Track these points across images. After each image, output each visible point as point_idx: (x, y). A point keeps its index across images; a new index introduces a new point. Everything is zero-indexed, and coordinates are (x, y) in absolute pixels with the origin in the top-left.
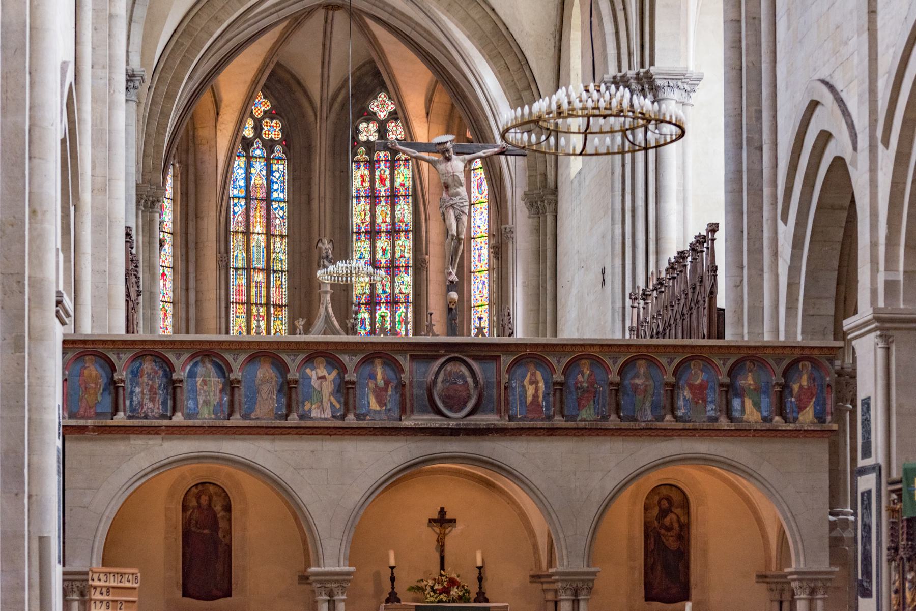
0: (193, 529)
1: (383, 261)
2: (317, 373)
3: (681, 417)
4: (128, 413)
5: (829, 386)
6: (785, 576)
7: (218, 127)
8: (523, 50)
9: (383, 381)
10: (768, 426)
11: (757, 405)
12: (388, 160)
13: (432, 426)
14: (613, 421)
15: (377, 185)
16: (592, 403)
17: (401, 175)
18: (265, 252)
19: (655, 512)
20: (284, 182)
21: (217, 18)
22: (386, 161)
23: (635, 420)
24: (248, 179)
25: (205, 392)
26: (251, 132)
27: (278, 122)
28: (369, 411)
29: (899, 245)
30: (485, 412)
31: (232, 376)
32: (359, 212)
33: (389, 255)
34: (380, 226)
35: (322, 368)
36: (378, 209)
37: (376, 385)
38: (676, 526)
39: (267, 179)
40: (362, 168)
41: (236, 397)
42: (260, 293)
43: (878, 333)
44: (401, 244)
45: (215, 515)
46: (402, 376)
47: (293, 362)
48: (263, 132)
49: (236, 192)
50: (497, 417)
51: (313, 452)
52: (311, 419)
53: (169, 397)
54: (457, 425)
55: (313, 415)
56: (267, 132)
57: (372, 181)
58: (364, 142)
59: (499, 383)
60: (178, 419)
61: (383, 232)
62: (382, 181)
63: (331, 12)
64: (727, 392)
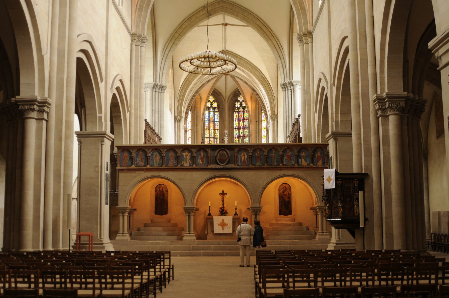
0: (158, 196)
1: (241, 135)
2: (185, 154)
3: (284, 164)
4: (135, 165)
5: (326, 155)
6: (316, 208)
7: (201, 104)
8: (269, 81)
9: (203, 156)
10: (309, 166)
11: (306, 161)
13: (216, 168)
14: (266, 166)
16: (260, 161)
19: (282, 191)
21: (195, 76)
22: (242, 111)
23: (272, 165)
24: (209, 116)
25: (156, 159)
28: (199, 164)
29: (339, 113)
30: (231, 164)
31: (163, 155)
32: (236, 124)
33: (243, 134)
35: (187, 153)
37: (201, 157)
38: (288, 194)
40: (236, 113)
41: (164, 160)
43: (333, 138)
45: (164, 192)
46: (208, 154)
47: (179, 151)
50: (234, 165)
51: (184, 175)
52: (184, 166)
53: (146, 161)
54: (223, 167)
55: (184, 165)
57: (239, 116)
58: (237, 107)
59: (234, 156)
60: (148, 166)
62: (241, 116)
63: (226, 76)
64: (297, 157)
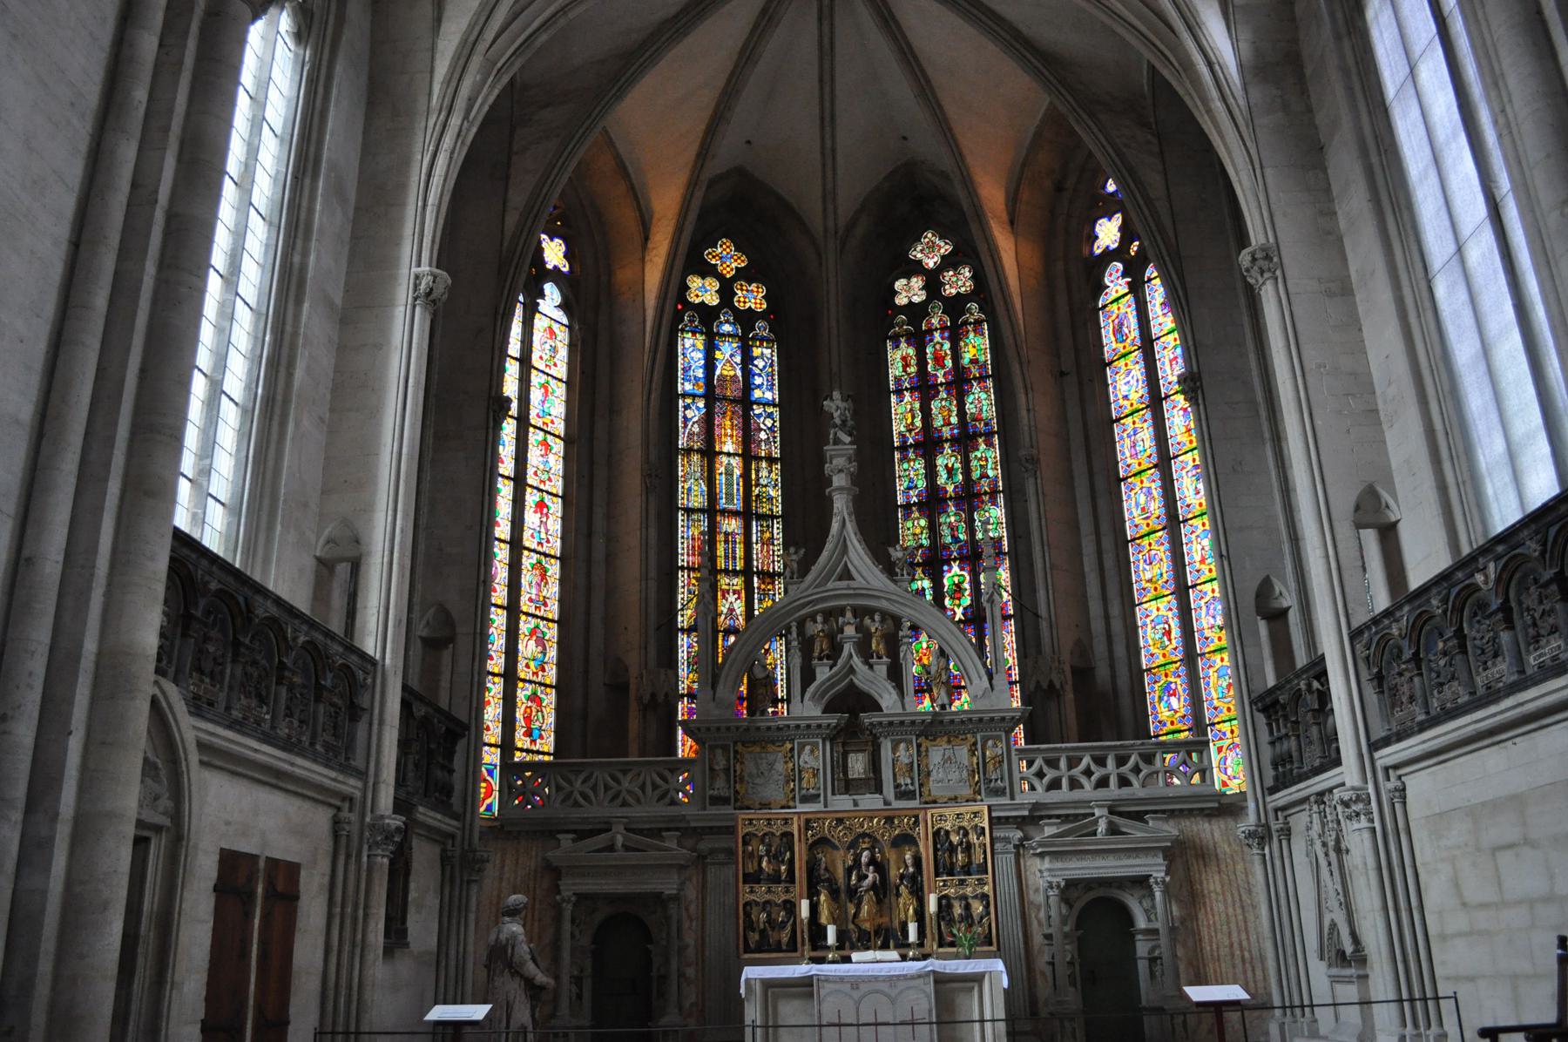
1: (950, 488)
7: (647, 258)
12: (947, 327)
15: (930, 368)
17: (970, 346)
18: (741, 484)
20: (773, 375)
22: (943, 329)
32: (903, 414)
34: (940, 431)
39: (743, 370)
40: (903, 345)
42: (734, 552)
44: (979, 456)
48: (735, 299)
49: (688, 387)
57: (922, 362)
61: (947, 440)
62: (939, 360)
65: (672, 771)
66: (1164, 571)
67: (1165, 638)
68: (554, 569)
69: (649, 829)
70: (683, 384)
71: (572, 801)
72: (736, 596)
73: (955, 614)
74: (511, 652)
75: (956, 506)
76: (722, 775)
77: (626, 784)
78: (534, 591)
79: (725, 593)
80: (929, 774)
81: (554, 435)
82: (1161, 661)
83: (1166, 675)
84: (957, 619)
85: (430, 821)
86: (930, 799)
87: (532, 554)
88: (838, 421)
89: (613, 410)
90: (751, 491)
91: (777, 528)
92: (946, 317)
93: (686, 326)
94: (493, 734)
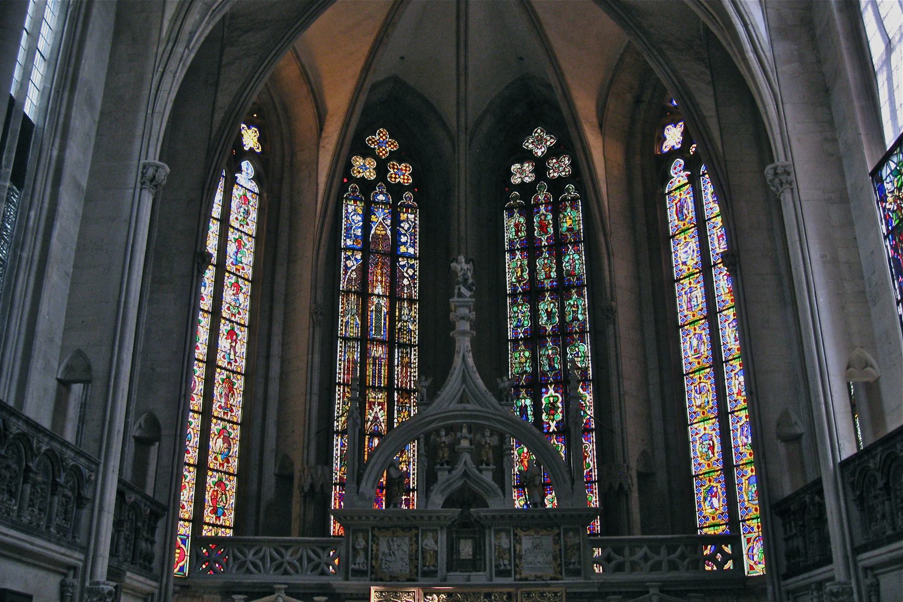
1: (549, 328)
7: (321, 144)
17: (568, 218)
18: (387, 319)
20: (415, 235)
24: (367, 225)
26: (372, 174)
27: (408, 165)
36: (539, 263)
40: (516, 215)
42: (380, 372)
49: (349, 242)
56: (393, 176)
61: (547, 290)
62: (543, 228)
65: (324, 549)
66: (710, 400)
67: (710, 452)
68: (239, 383)
69: (304, 594)
70: (345, 240)
71: (244, 569)
72: (380, 407)
73: (550, 426)
74: (204, 448)
75: (553, 342)
76: (362, 553)
77: (288, 558)
78: (223, 400)
79: (372, 404)
80: (520, 557)
81: (244, 279)
82: (706, 469)
83: (710, 481)
84: (551, 430)
85: (136, 584)
86: (524, 575)
87: (223, 371)
88: (460, 279)
89: (291, 259)
90: (395, 325)
91: (414, 358)
92: (550, 195)
93: (350, 195)
94: (187, 511)
